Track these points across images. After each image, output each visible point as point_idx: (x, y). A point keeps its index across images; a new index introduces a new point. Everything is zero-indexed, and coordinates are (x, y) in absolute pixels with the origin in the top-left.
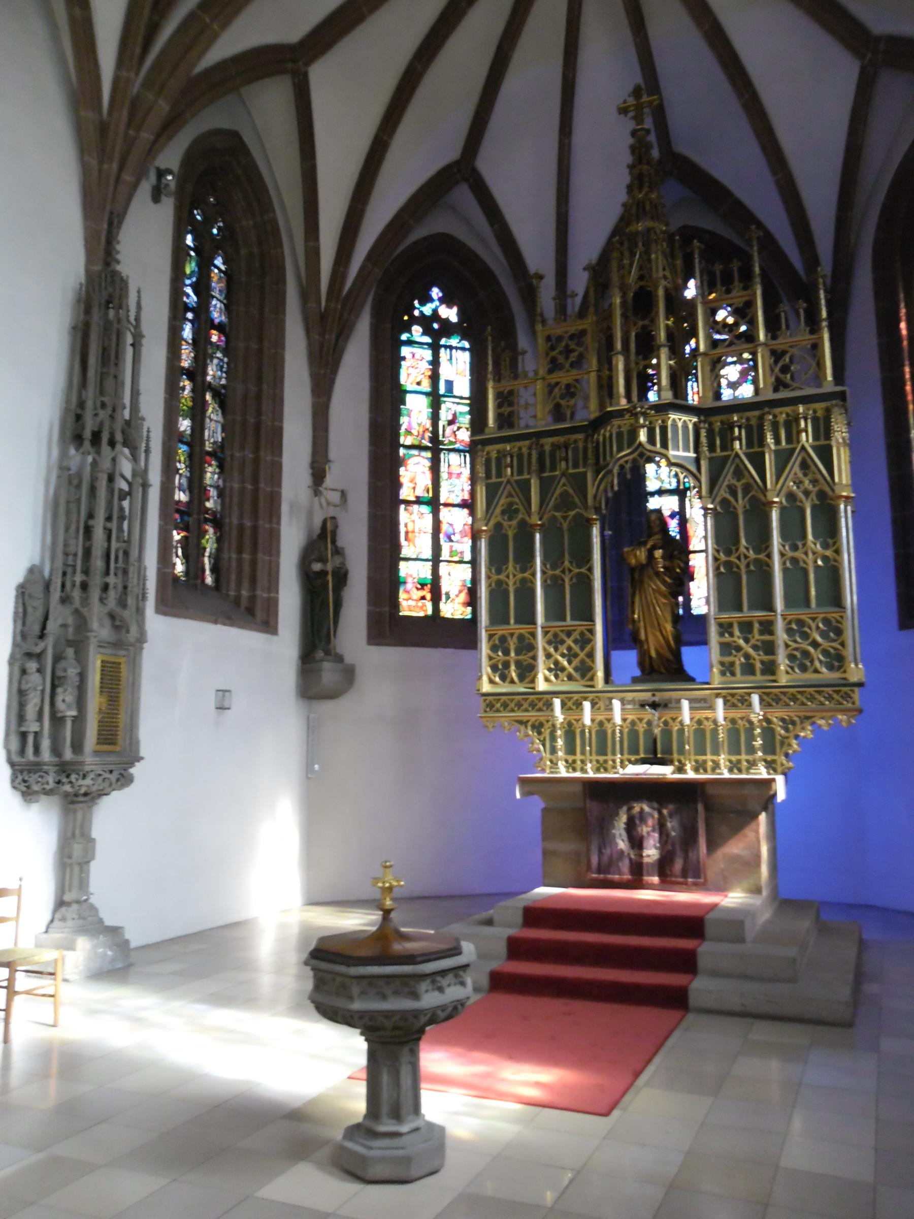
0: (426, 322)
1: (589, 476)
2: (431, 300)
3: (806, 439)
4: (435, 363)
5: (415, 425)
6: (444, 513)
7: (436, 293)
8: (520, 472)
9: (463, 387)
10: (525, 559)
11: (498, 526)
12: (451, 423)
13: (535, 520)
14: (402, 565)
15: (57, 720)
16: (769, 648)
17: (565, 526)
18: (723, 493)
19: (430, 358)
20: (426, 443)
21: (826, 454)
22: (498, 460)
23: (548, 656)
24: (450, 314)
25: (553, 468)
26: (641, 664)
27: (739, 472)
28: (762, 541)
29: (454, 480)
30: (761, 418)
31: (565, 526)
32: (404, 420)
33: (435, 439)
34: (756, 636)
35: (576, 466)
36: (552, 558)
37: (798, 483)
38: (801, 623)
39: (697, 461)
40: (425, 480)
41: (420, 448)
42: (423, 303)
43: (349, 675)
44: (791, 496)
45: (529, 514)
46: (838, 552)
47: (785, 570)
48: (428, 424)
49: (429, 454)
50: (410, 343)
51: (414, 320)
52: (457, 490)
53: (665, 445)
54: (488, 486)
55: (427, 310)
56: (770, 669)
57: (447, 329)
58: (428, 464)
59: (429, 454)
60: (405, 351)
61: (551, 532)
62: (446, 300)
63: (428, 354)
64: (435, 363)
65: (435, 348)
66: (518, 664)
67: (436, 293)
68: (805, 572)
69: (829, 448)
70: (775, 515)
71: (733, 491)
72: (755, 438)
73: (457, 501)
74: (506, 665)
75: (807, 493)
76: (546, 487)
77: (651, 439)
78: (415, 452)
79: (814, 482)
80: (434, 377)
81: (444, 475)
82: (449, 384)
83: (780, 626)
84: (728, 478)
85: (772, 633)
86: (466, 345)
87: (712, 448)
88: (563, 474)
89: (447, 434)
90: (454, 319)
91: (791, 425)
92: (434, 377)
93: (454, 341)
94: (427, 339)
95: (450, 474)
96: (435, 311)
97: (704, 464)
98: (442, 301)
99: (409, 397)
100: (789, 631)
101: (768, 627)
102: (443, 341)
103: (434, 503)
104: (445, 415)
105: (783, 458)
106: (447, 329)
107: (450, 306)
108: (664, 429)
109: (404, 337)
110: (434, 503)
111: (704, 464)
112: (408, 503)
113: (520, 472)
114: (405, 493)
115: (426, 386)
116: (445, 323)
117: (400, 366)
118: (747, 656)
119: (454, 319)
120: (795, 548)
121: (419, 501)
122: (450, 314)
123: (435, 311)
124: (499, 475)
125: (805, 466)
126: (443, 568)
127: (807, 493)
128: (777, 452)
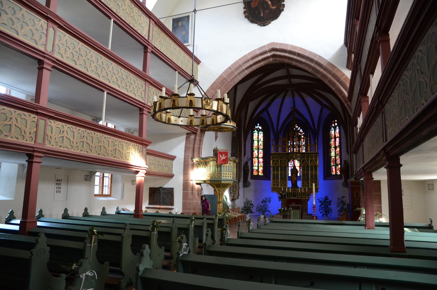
0: (257, 129)
1: (287, 160)
2: (258, 126)
3: (314, 159)
4: (258, 136)
5: (255, 146)
6: (259, 159)
7: (258, 124)
8: (277, 159)
9: (262, 139)
10: (278, 171)
11: (274, 166)
12: (260, 145)
13: (279, 165)
14: (254, 167)
15: (234, 191)
16: (308, 183)
17: (283, 166)
18: (303, 164)
19: (257, 135)
20: (257, 148)
21: (316, 161)
22: (274, 157)
23: (280, 183)
24: (260, 128)
25: (282, 159)
26: (292, 185)
27: (305, 162)
28: (308, 171)
29: (261, 154)
30: (308, 155)
31: (283, 166)
32: (254, 145)
33: (258, 148)
34: (307, 182)
35: (285, 159)
36: (281, 171)
37: (313, 164)
38: (312, 181)
39: (301, 160)
40: (257, 154)
41: (256, 149)
42: (257, 126)
43: (250, 183)
44: (312, 165)
45: (278, 164)
46: (317, 172)
47: (310, 174)
48: (257, 145)
49: (257, 150)
50: (255, 133)
51: (255, 129)
52: (261, 155)
53: (297, 158)
54: (273, 161)
55: (257, 127)
56: (308, 186)
57: (260, 130)
58: (257, 151)
59: (257, 150)
60: (254, 134)
61: (281, 167)
62: (260, 126)
63: (257, 134)
64: (258, 136)
65: (258, 133)
66: (276, 184)
67: (258, 124)
68: (313, 174)
69: (316, 160)
70: (310, 168)
71: (305, 164)
72: (308, 158)
73: (261, 157)
74: (275, 184)
75: (314, 165)
76: (281, 161)
77: (295, 157)
78: (255, 150)
79: (314, 164)
80: (258, 138)
81: (259, 153)
82: (260, 139)
83: (310, 181)
84: (304, 163)
85: (309, 182)
86: (262, 132)
87: (302, 158)
88: (283, 160)
89: (260, 146)
90: (261, 129)
91: (312, 156)
92: (258, 138)
93: (261, 132)
94: (257, 132)
95: (260, 153)
96: (258, 128)
97: (301, 160)
98: (259, 126)
99: (255, 141)
100: (311, 182)
101: (308, 181)
102: (259, 132)
103: (258, 158)
104: (260, 144)
105: (311, 161)
106: (260, 130)
107: (260, 127)
108: (297, 156)
109: (254, 132)
110: (258, 158)
111: (301, 160)
112: (255, 158)
113: (277, 159)
114: (254, 156)
115: (257, 140)
116: (260, 129)
117: (253, 137)
118: (306, 184)
119: (261, 129)
120: (312, 172)
121: (256, 157)
122: (260, 128)
123: (258, 128)
124: (274, 159)
125: (313, 162)
126: (259, 167)
127: (314, 165)
128: (310, 160)
